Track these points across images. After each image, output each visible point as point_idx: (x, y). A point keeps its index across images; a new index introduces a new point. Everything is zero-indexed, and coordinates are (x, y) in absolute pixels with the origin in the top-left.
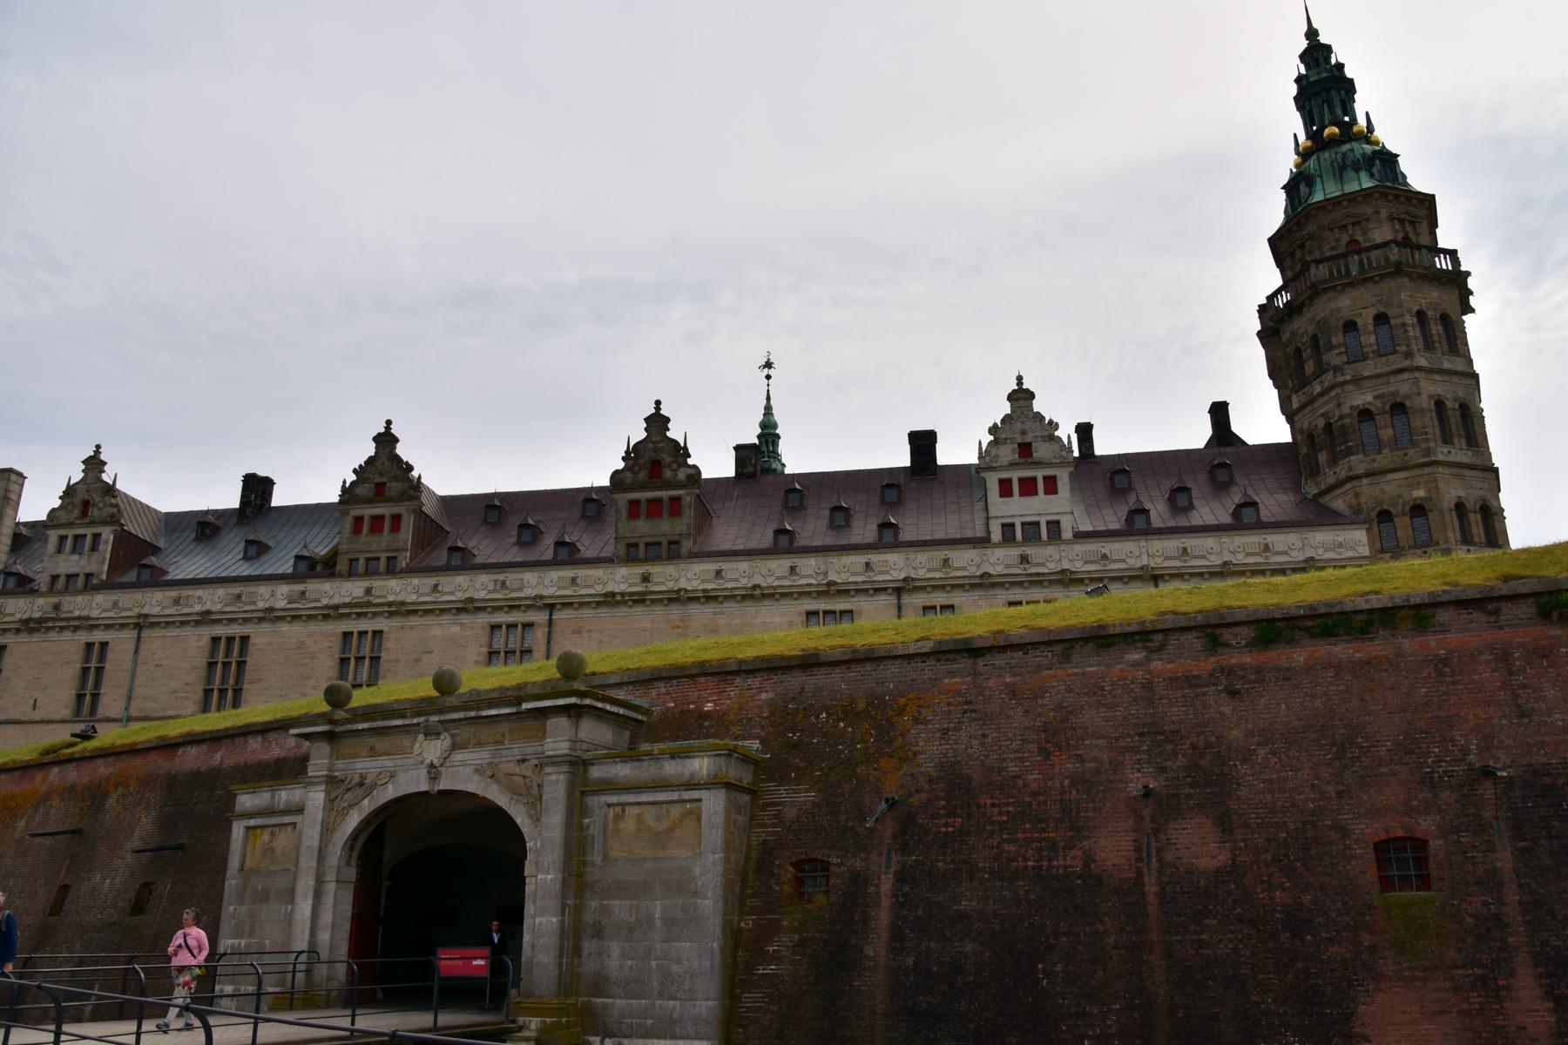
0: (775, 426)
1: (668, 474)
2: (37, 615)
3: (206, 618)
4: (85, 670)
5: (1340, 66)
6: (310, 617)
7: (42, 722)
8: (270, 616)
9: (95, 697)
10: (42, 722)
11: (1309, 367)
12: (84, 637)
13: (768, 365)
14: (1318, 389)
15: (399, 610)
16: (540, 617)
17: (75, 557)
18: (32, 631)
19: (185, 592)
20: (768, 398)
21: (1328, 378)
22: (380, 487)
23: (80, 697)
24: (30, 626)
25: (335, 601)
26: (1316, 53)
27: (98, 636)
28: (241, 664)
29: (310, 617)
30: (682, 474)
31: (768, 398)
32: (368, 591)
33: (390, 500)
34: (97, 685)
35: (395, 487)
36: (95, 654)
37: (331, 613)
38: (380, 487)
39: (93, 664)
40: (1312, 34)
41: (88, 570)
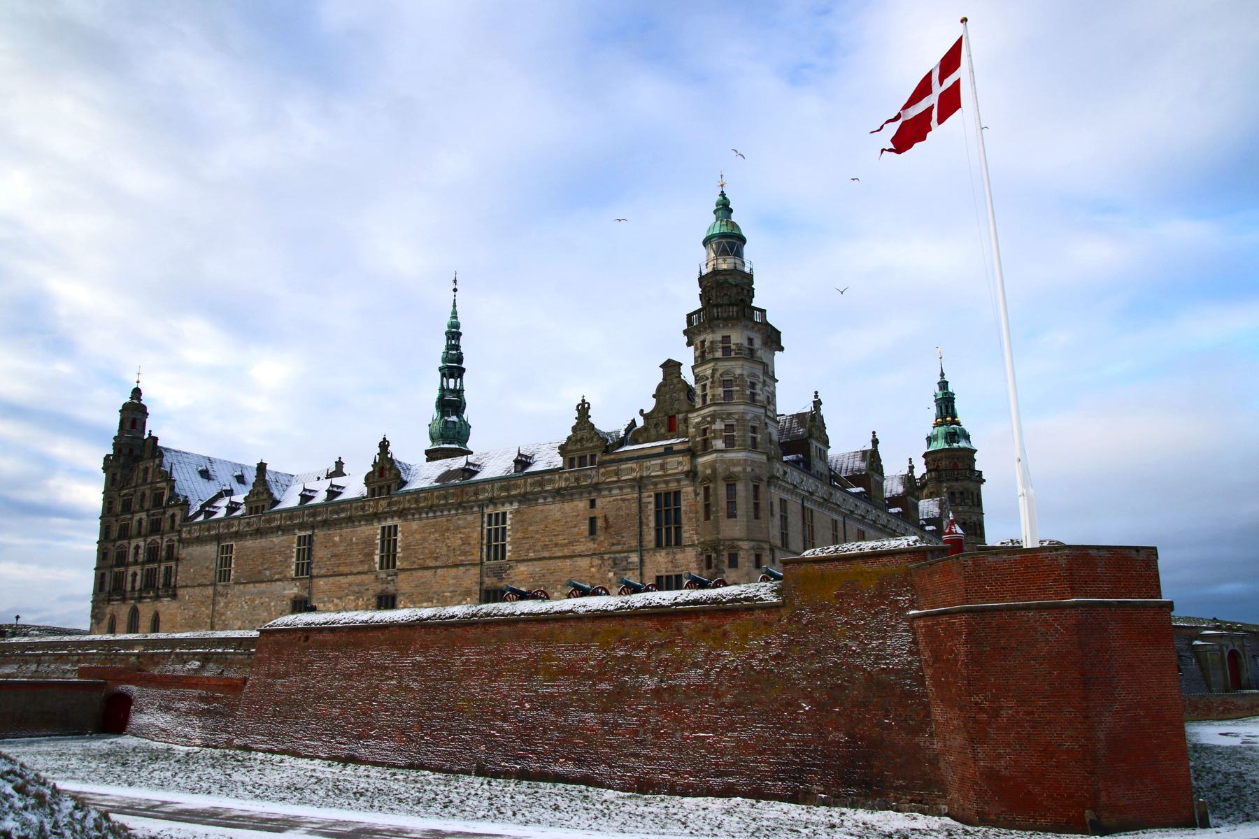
0: (457, 326)
11: (958, 501)
13: (455, 281)
20: (455, 306)
21: (966, 508)
26: (943, 385)
31: (455, 306)
40: (942, 375)
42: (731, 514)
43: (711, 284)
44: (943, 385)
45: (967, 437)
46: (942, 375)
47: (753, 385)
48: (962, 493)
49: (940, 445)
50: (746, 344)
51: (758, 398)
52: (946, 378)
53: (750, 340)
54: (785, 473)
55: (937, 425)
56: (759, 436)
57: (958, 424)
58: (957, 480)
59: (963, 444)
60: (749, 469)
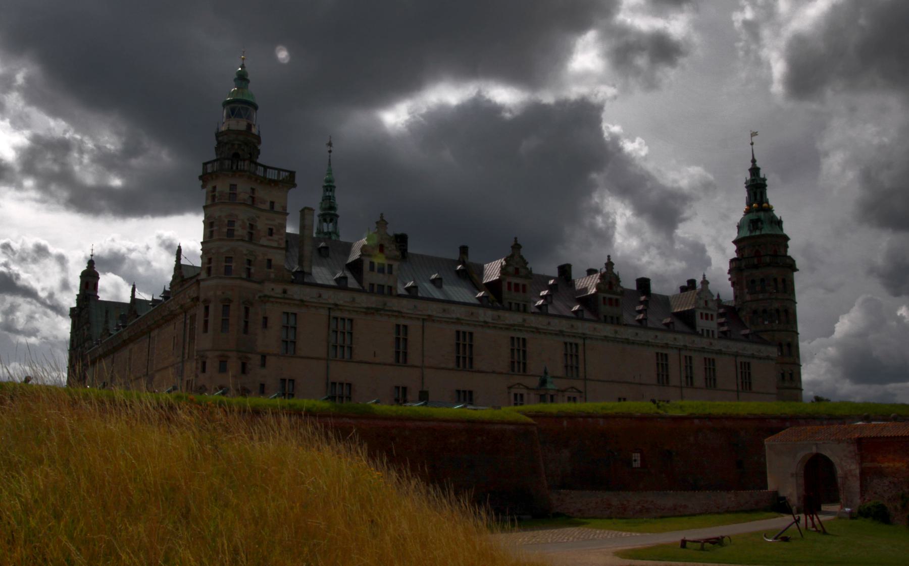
1: (614, 288)
2: (374, 306)
3: (458, 321)
4: (398, 339)
5: (764, 180)
6: (501, 328)
7: (379, 364)
8: (486, 324)
9: (405, 354)
10: (379, 364)
12: (394, 321)
14: (761, 296)
15: (538, 331)
16: (580, 342)
17: (381, 275)
18: (366, 313)
19: (446, 306)
22: (517, 270)
23: (398, 353)
24: (370, 311)
25: (512, 322)
26: (755, 171)
27: (402, 322)
28: (471, 346)
29: (501, 328)
30: (619, 290)
32: (524, 320)
33: (521, 277)
34: (406, 348)
35: (522, 271)
36: (401, 333)
37: (509, 327)
38: (517, 270)
39: (401, 336)
40: (754, 161)
41: (390, 284)
42: (206, 330)
43: (223, 140)
44: (755, 171)
45: (779, 223)
46: (754, 161)
47: (231, 223)
48: (762, 280)
49: (746, 233)
50: (227, 190)
51: (236, 233)
52: (758, 164)
53: (233, 187)
54: (285, 292)
55: (747, 212)
56: (233, 265)
57: (769, 209)
58: (756, 267)
59: (766, 230)
60: (219, 293)
